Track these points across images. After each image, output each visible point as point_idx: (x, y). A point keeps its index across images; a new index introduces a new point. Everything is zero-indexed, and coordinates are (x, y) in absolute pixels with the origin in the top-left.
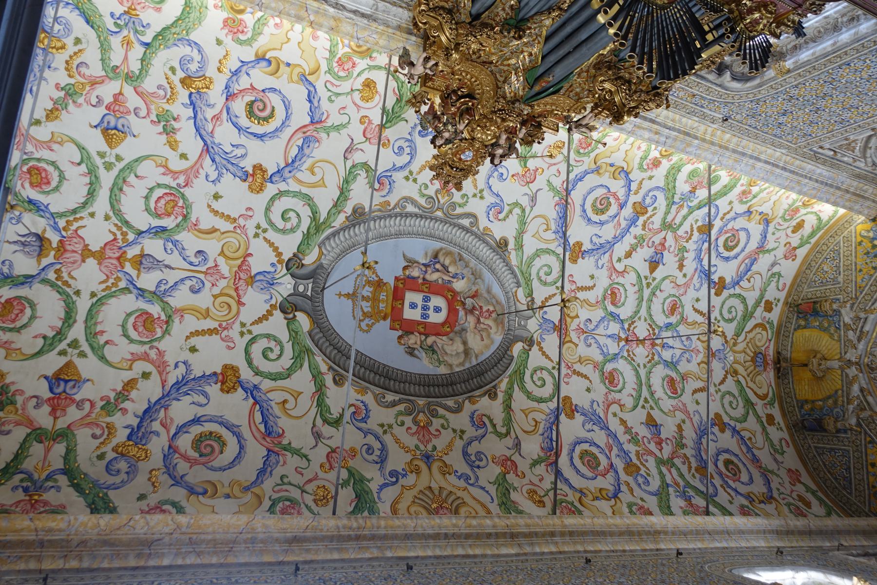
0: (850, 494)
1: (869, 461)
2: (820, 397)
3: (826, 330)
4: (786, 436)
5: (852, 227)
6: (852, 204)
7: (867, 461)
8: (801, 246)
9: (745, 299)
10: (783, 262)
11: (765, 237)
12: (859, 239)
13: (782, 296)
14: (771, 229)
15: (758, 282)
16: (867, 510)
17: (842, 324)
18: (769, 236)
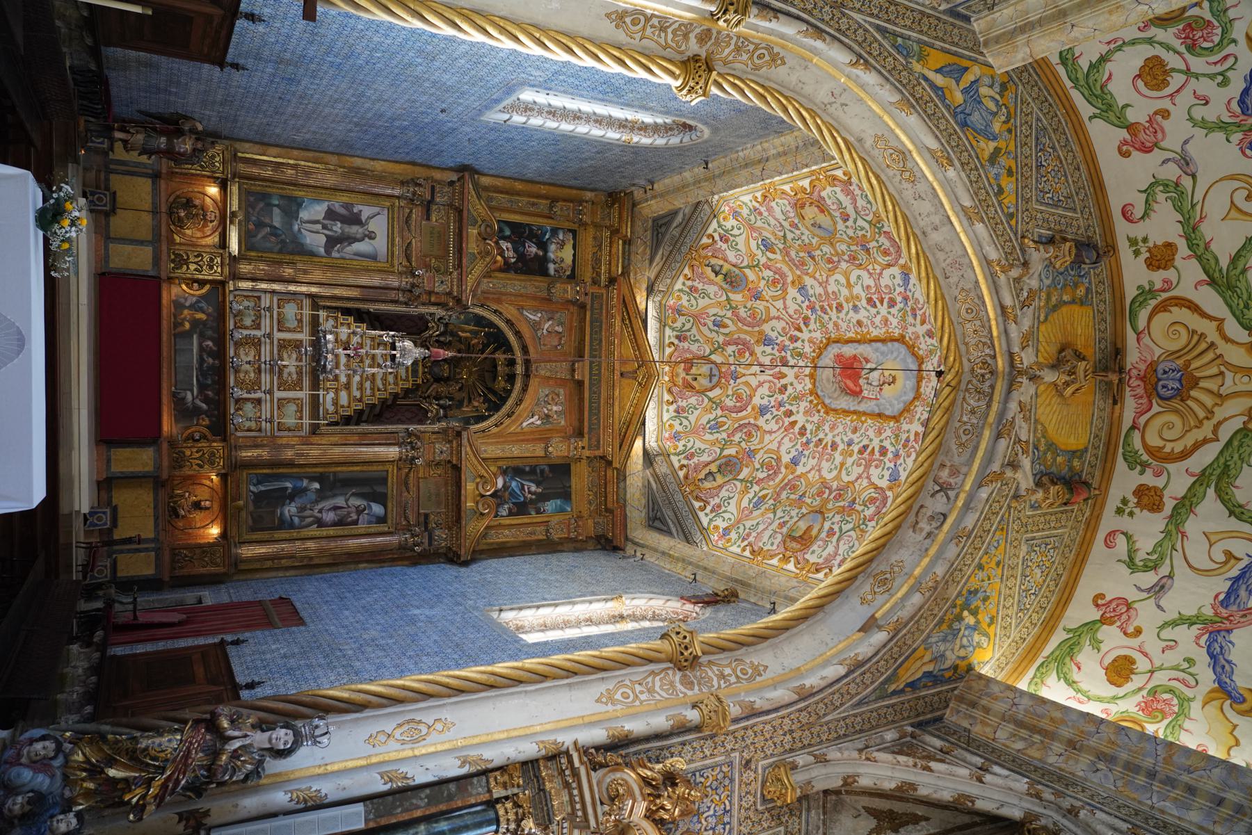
0: (1038, 119)
1: (1014, 179)
2: (1064, 309)
3: (1051, 446)
4: (1122, 229)
5: (997, 656)
6: (1040, 710)
7: (1017, 179)
8: (1091, 626)
9: (1232, 513)
10: (1132, 594)
11: (1212, 656)
12: (991, 631)
13: (1109, 521)
14: (1207, 678)
15: (1197, 550)
16: (1020, 87)
17: (1031, 454)
18: (1202, 657)
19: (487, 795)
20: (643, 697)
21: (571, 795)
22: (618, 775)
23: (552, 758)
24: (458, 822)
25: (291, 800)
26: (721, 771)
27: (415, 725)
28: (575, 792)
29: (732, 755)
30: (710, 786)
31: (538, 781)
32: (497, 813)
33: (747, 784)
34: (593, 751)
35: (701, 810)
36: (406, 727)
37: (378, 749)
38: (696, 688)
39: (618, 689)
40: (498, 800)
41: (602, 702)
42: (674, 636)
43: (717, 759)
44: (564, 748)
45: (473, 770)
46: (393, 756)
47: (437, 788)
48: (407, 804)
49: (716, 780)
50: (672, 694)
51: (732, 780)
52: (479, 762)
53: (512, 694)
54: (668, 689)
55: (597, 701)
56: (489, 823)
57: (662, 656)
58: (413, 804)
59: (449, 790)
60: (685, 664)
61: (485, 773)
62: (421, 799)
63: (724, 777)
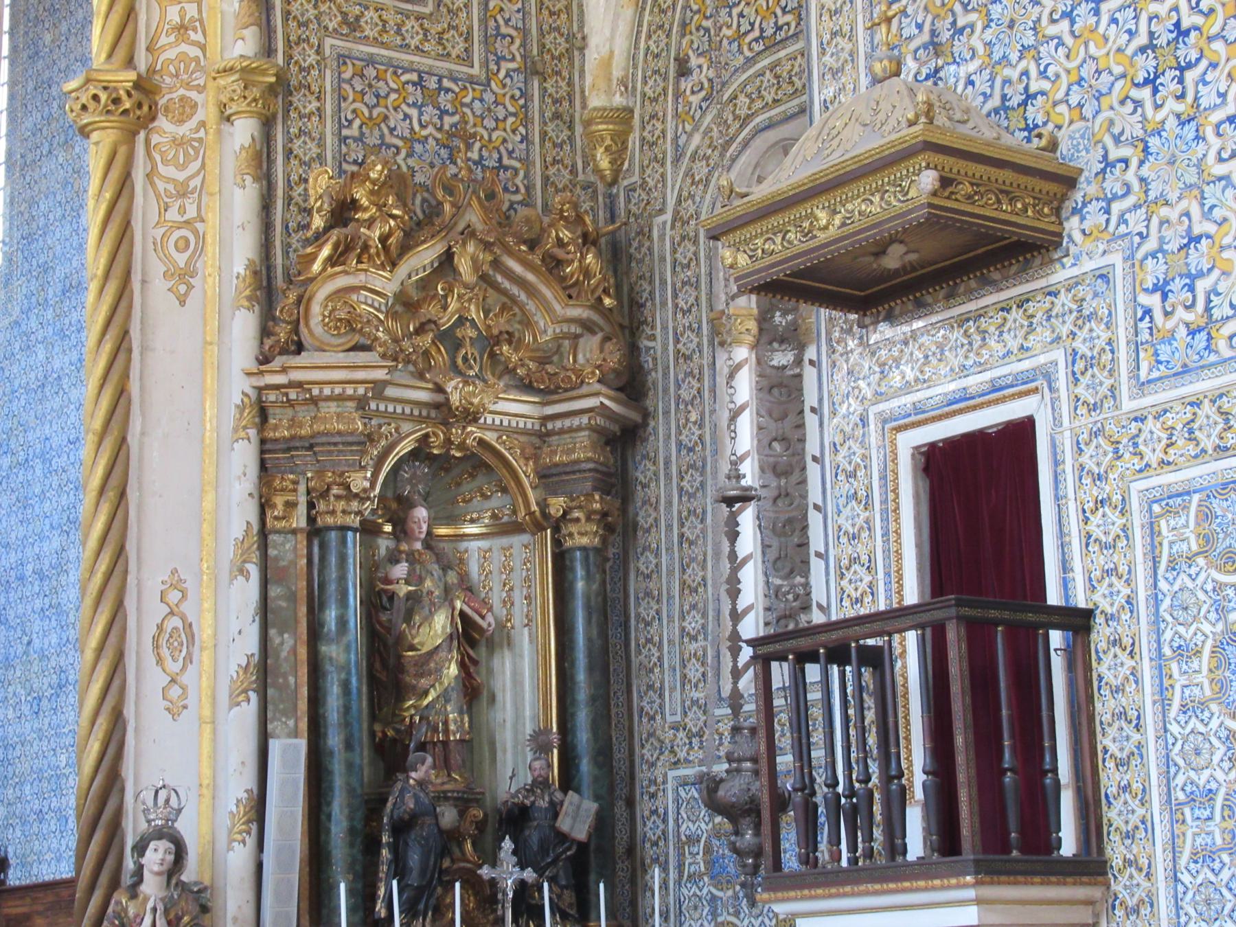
19: (299, 536)
20: (191, 212)
21: (329, 399)
22: (316, 308)
23: (263, 414)
24: (332, 588)
25: (244, 842)
26: (349, 82)
27: (165, 636)
28: (327, 391)
29: (327, 52)
30: (371, 108)
31: (296, 449)
32: (329, 528)
33: (384, 30)
34: (268, 342)
35: (407, 133)
36: (165, 652)
37: (191, 701)
38: (193, 95)
39: (168, 257)
40: (311, 520)
41: (186, 294)
42: (86, 119)
43: (328, 88)
44: (253, 394)
45: (255, 556)
46: (205, 683)
47: (270, 616)
48: (285, 667)
49: (363, 93)
50: (197, 151)
51: (371, 61)
52: (246, 545)
53: (141, 459)
54: (186, 154)
55: (182, 303)
56: (343, 541)
57: (122, 150)
58: (286, 659)
59: (279, 597)
60: (146, 108)
61: (264, 533)
62: (282, 643)
63: (362, 76)
